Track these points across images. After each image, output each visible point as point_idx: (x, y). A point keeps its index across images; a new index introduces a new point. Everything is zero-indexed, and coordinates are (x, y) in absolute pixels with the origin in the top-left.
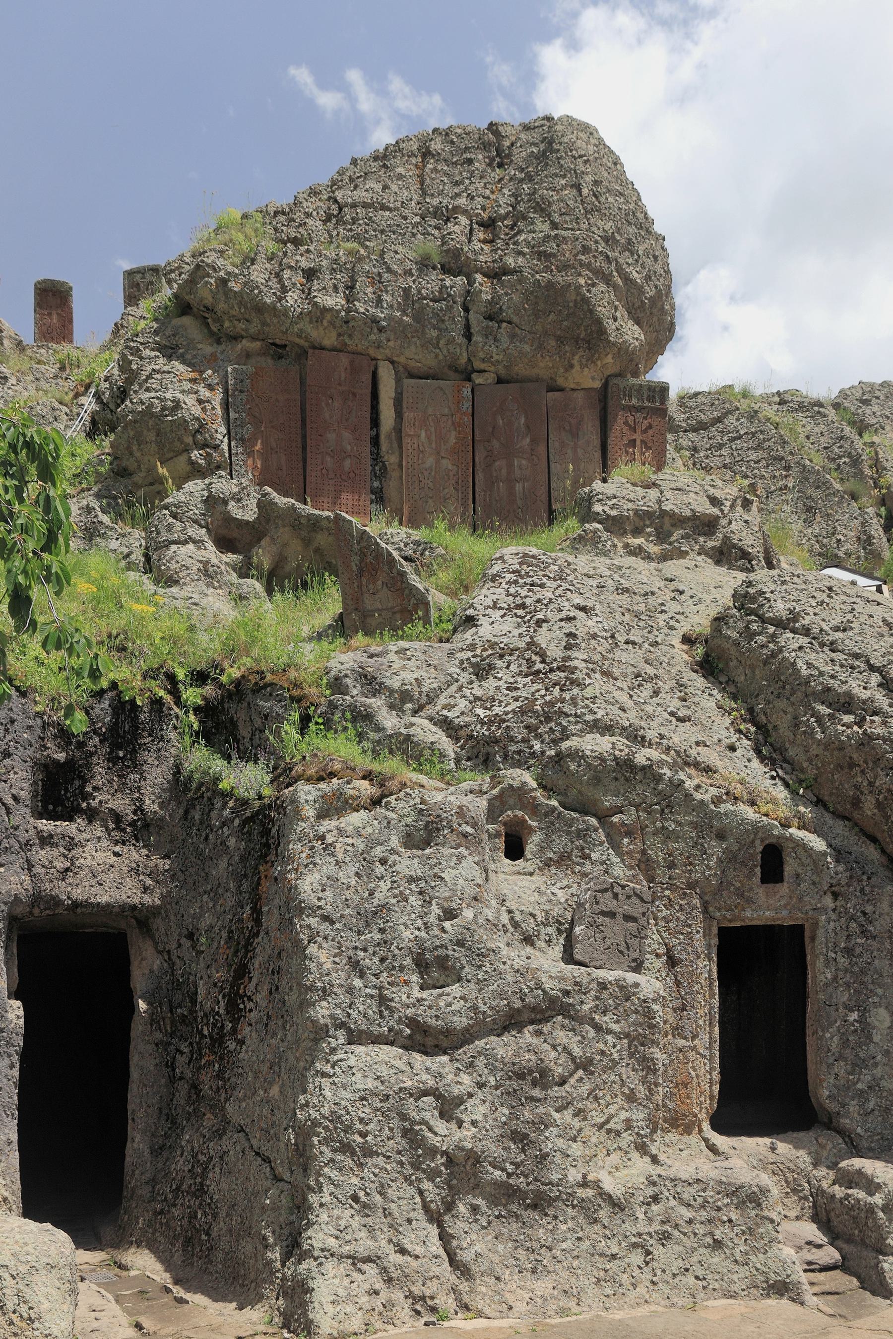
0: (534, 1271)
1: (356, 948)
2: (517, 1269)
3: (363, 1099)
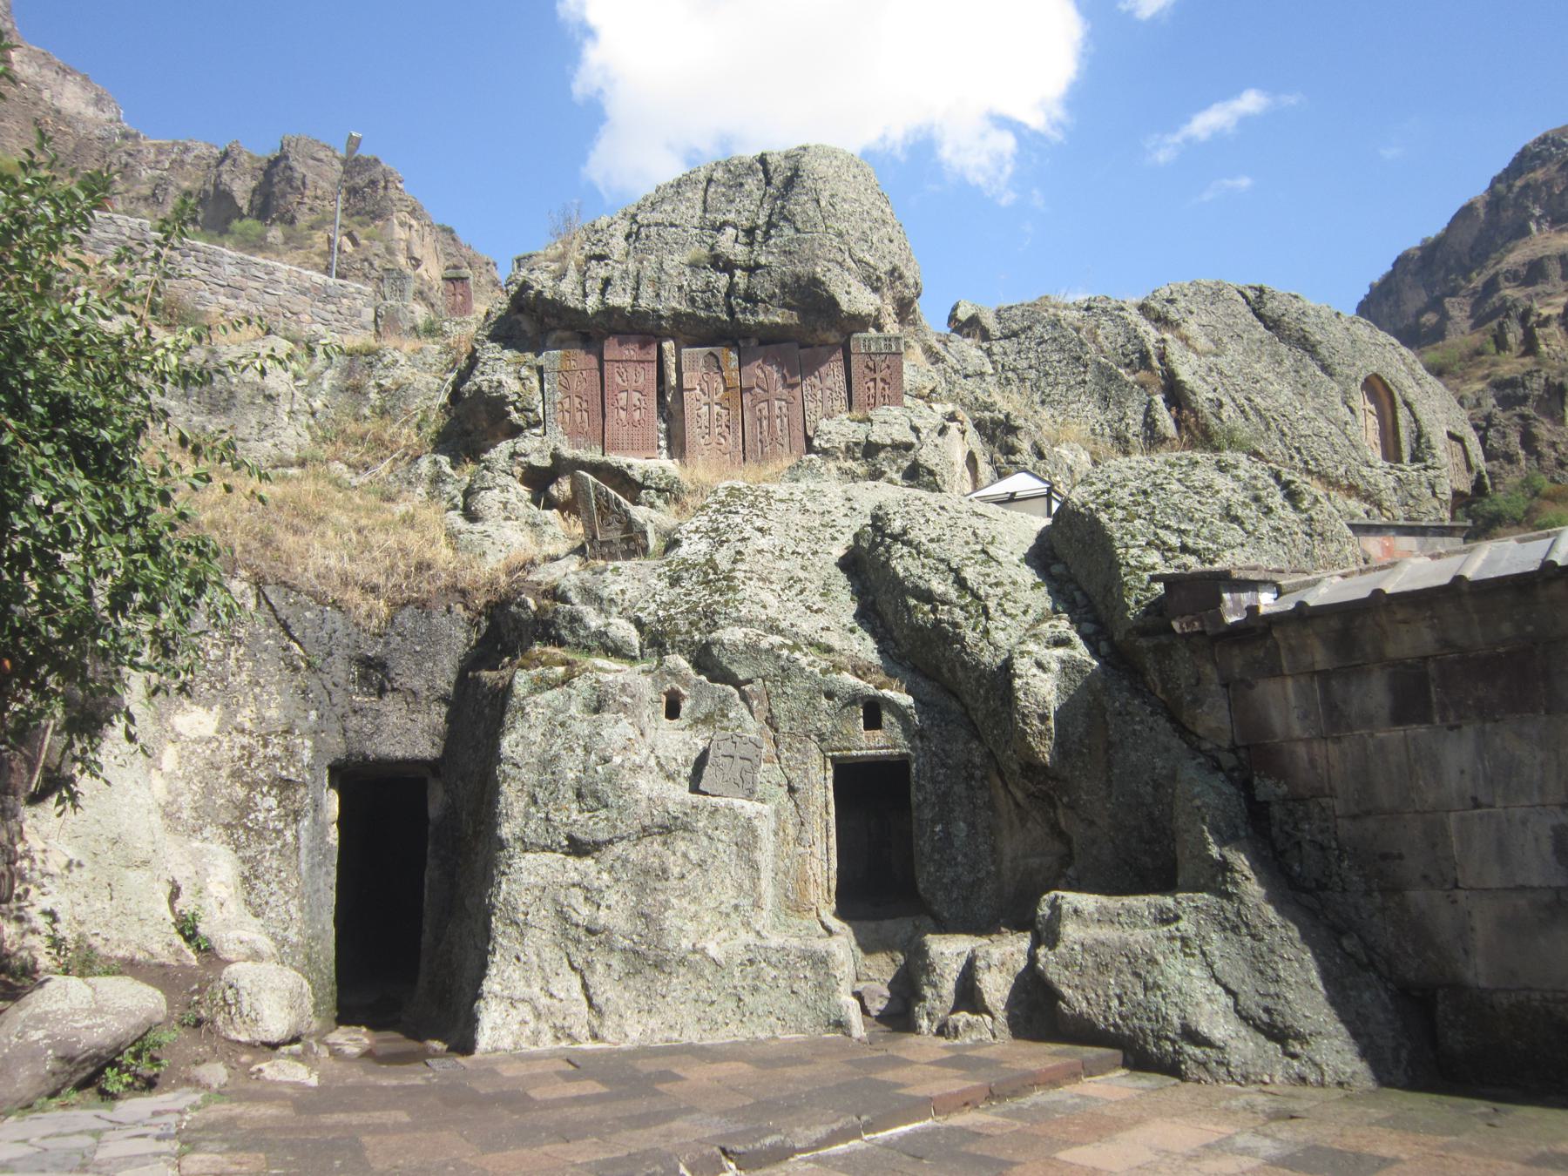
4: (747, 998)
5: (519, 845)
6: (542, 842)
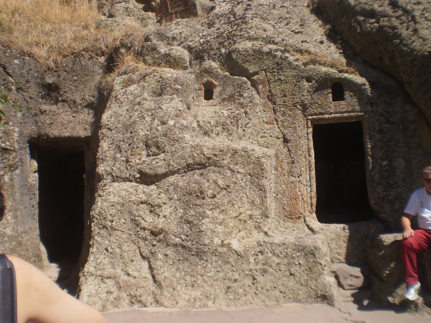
0: (193, 286)
1: (120, 141)
2: (185, 285)
3: (112, 206)
4: (260, 278)
5: (110, 177)
6: (124, 175)
